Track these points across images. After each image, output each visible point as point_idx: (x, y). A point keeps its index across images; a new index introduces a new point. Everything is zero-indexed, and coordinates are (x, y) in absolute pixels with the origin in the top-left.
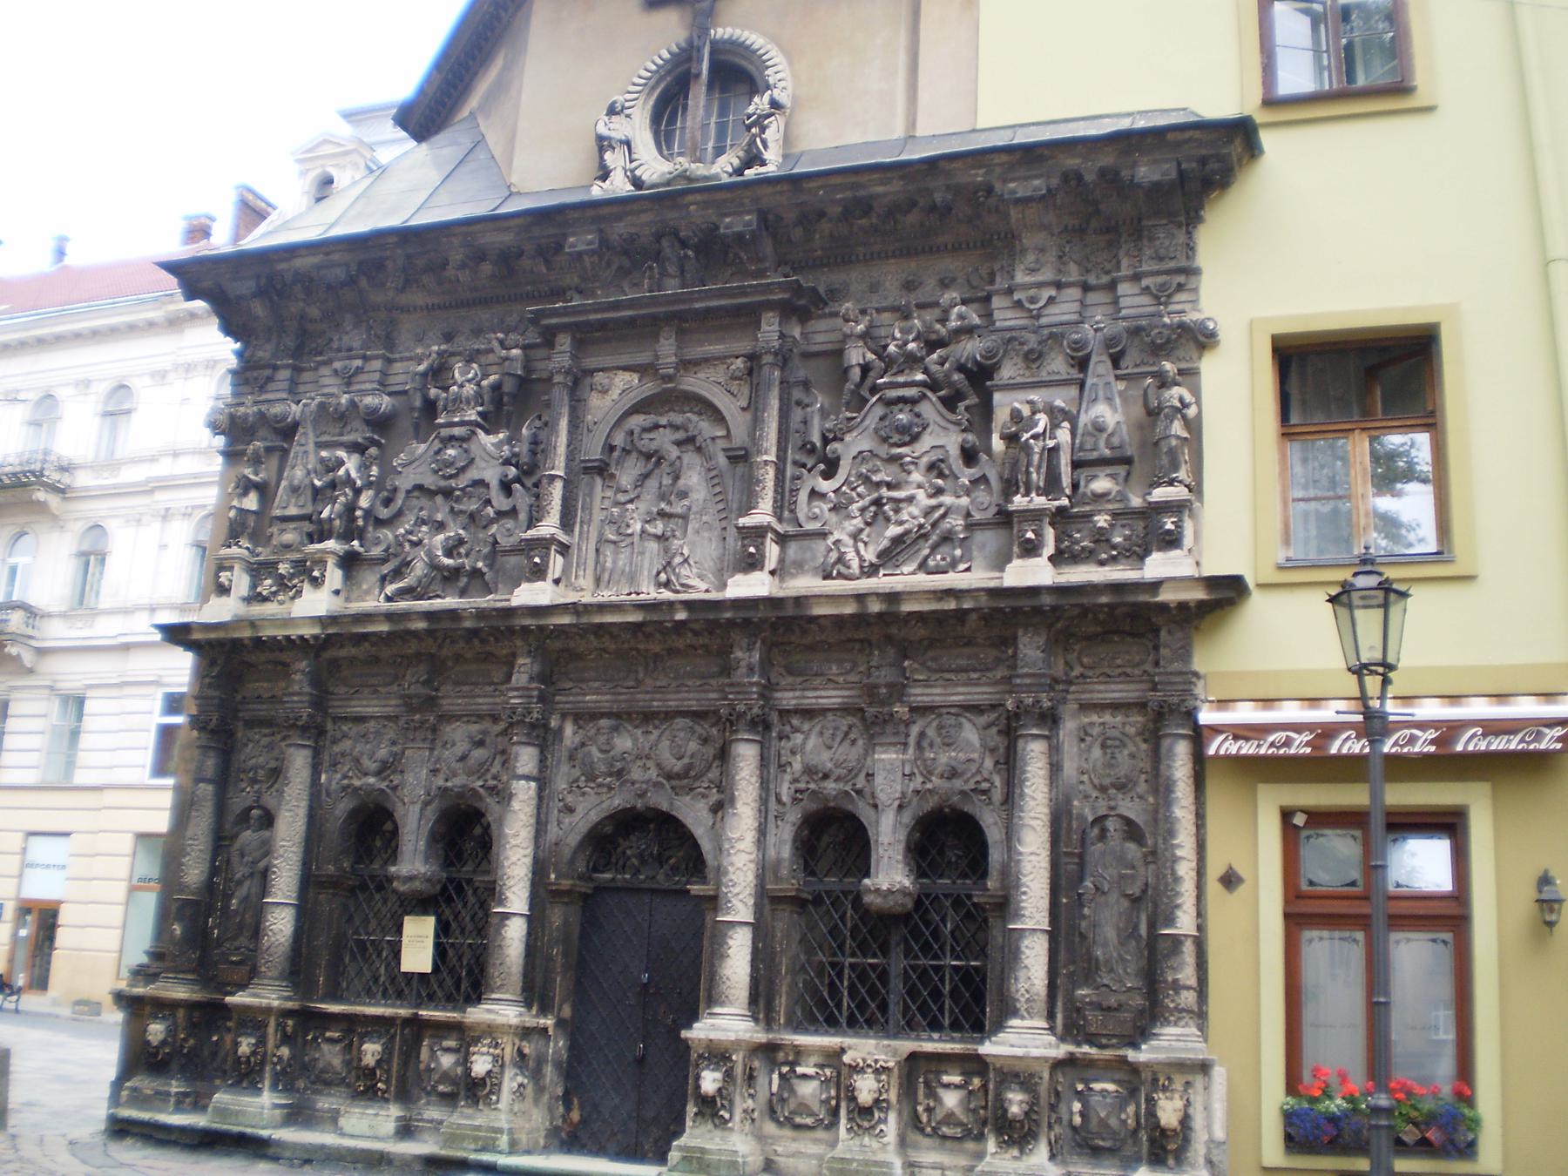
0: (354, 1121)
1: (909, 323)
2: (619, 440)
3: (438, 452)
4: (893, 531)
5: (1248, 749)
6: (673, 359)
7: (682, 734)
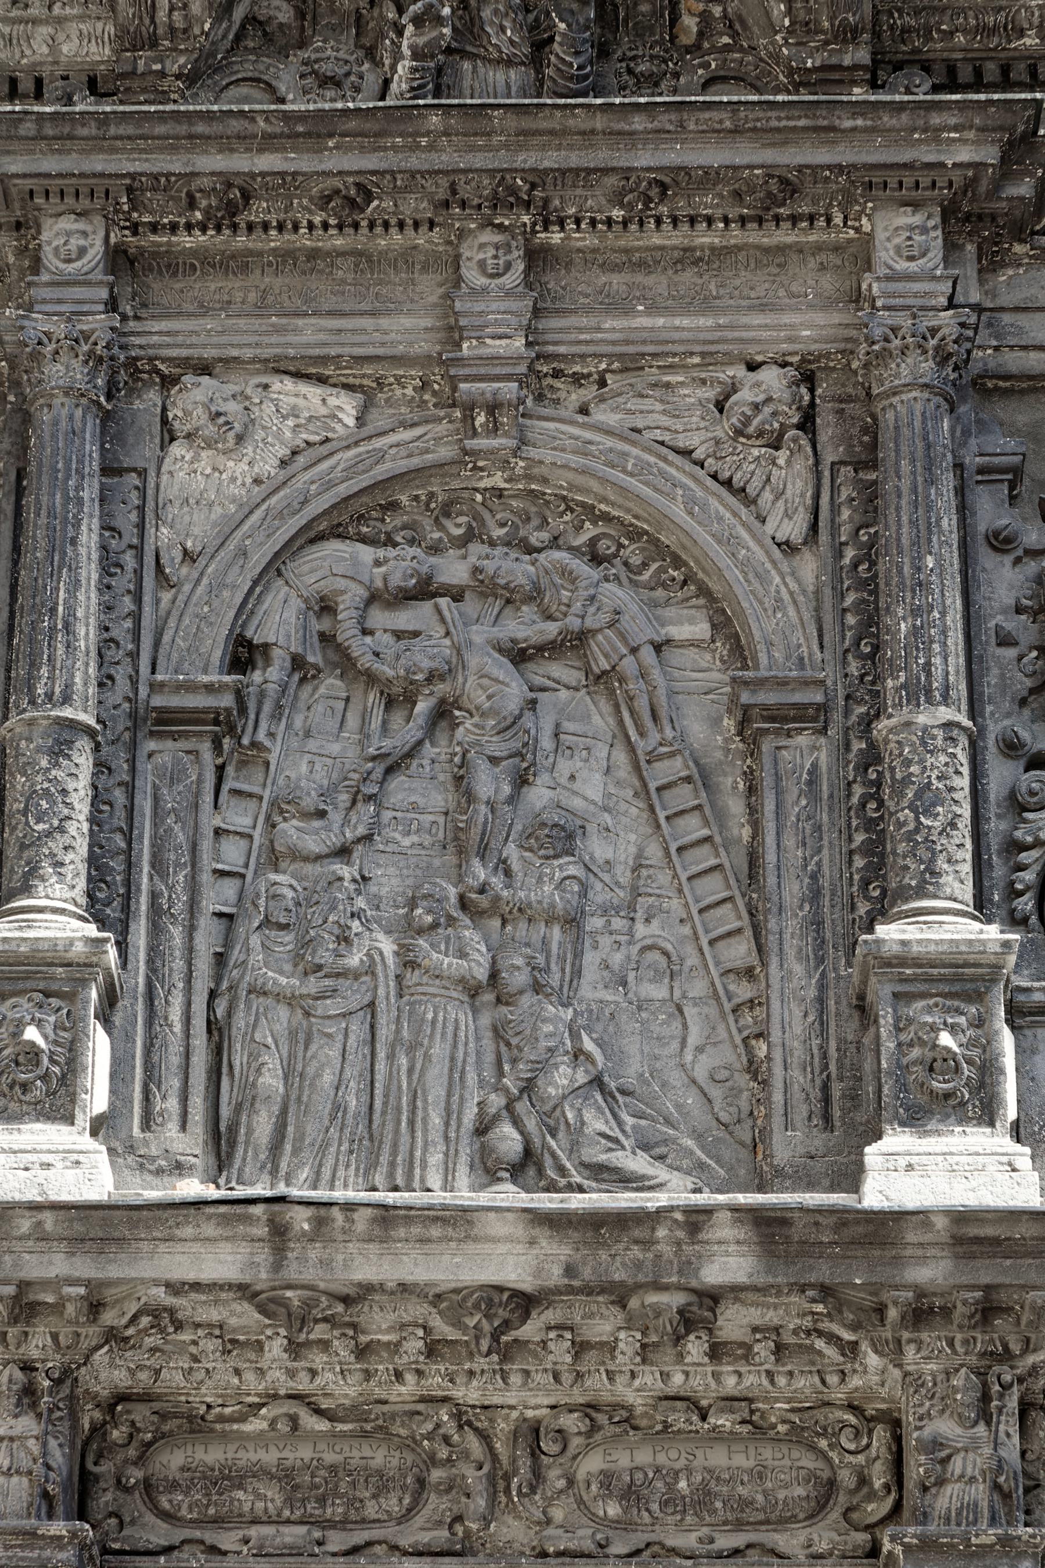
2: (280, 623)
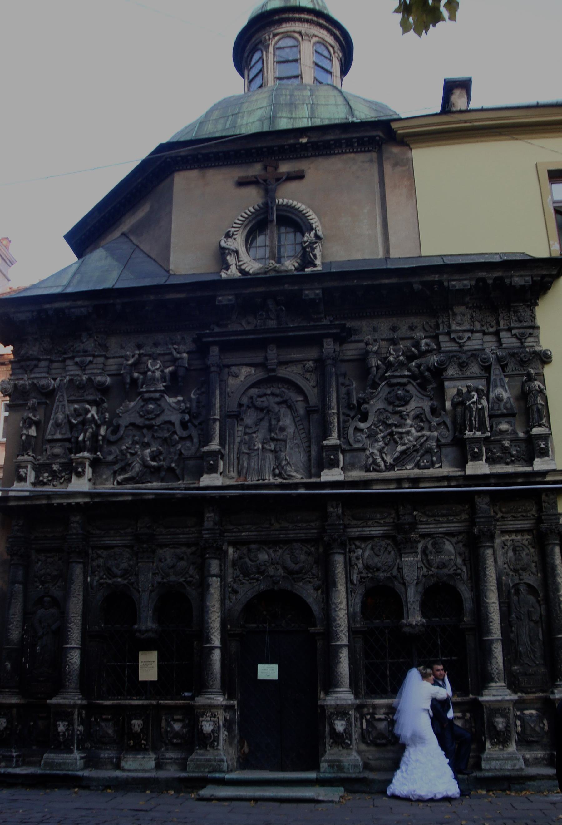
0: (130, 762)
1: (398, 347)
2: (245, 401)
3: (142, 407)
4: (400, 448)
6: (276, 361)
7: (297, 551)
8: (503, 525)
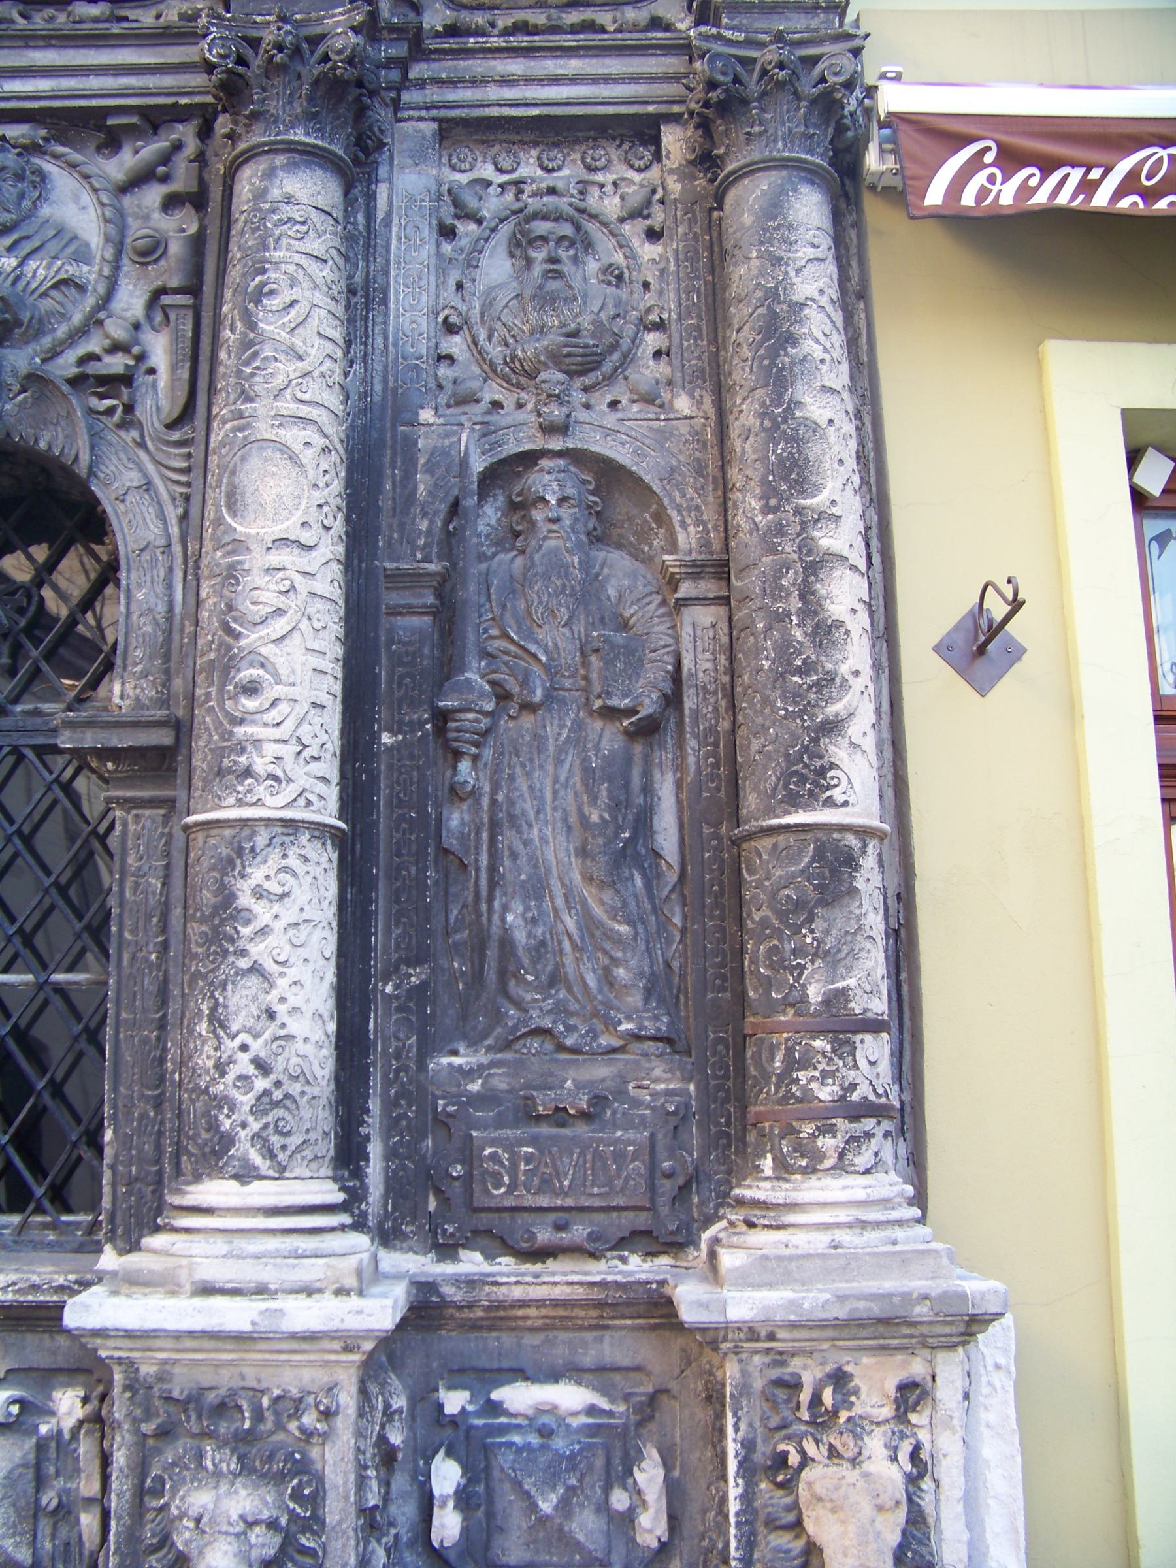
5: (1058, 190)
8: (453, 83)
